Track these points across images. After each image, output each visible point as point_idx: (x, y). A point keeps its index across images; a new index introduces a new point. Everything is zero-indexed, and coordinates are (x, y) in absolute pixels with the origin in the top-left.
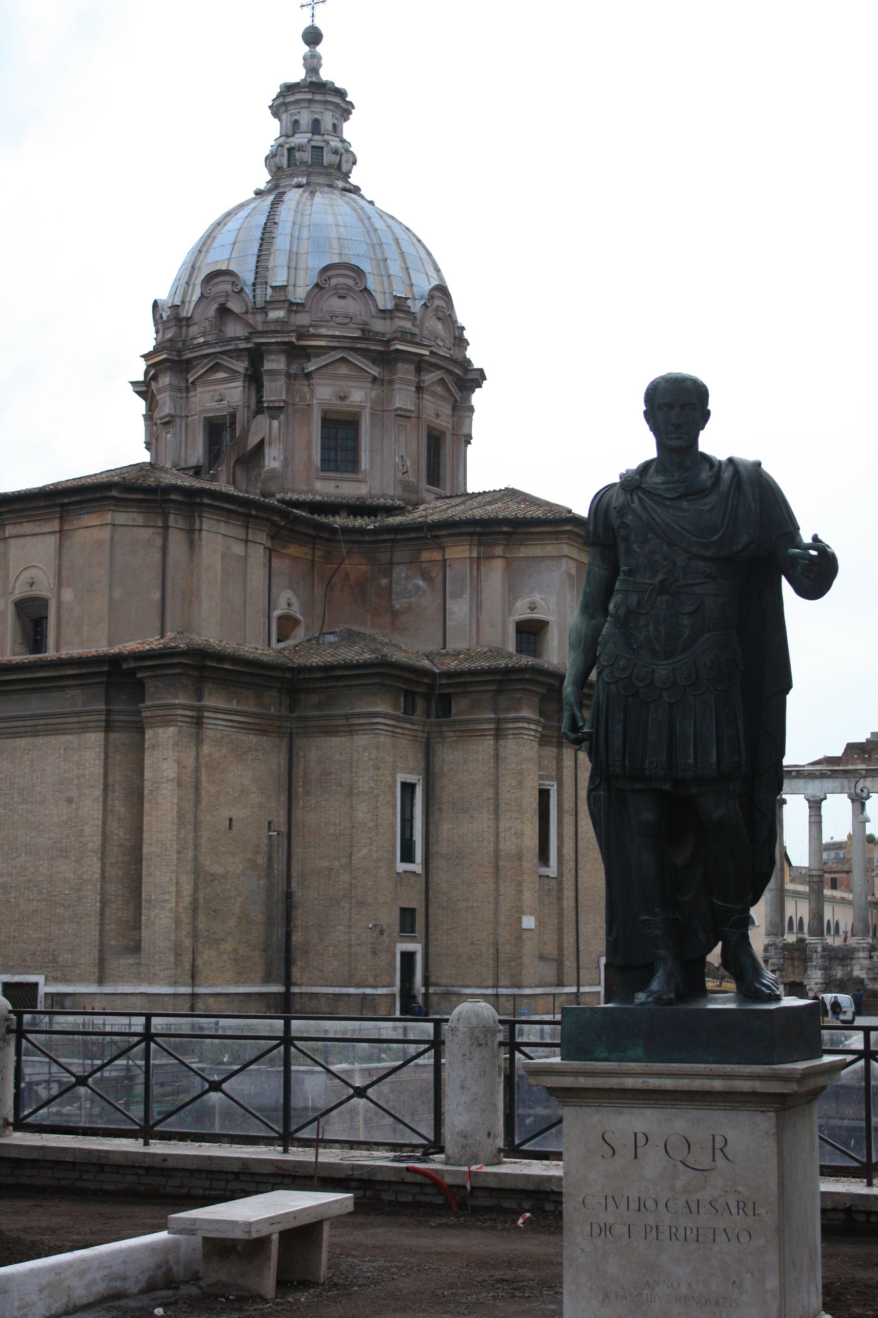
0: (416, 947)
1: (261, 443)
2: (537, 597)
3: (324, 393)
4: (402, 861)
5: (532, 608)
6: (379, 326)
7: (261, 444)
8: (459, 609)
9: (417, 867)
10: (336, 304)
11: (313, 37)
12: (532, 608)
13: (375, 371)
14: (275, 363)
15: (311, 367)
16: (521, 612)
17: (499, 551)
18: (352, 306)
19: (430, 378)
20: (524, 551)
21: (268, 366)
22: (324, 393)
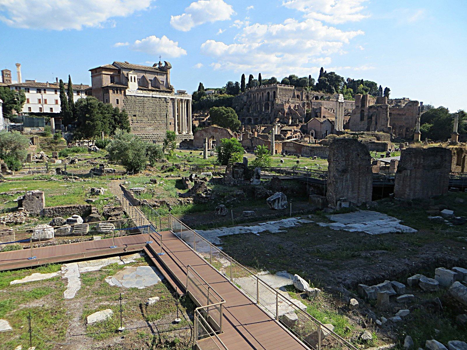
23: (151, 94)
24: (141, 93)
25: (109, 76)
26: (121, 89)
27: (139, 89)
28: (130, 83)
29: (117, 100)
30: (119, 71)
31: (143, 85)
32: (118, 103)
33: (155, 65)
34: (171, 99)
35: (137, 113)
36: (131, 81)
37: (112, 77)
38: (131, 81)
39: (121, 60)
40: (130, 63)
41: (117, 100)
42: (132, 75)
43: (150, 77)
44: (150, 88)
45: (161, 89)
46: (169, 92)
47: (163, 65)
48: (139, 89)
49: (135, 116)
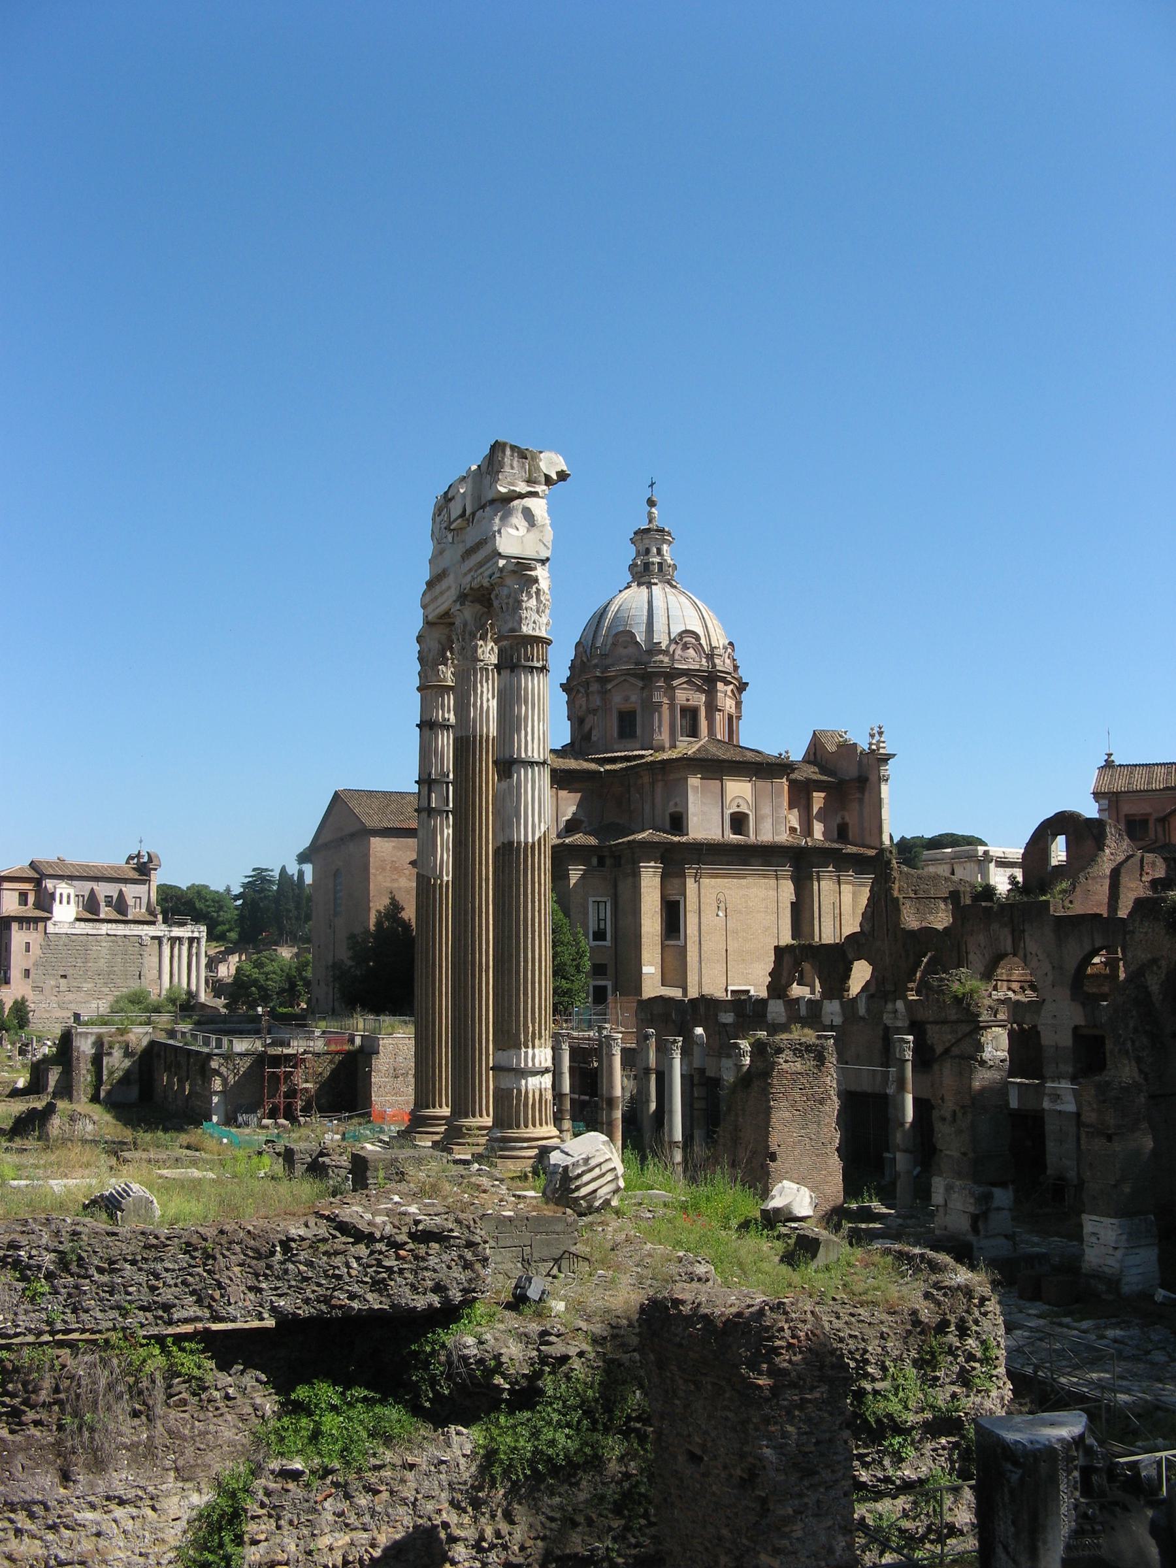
0: (609, 984)
1: (591, 729)
2: (677, 800)
3: (617, 700)
4: (605, 940)
5: (676, 804)
6: (645, 658)
7: (591, 729)
8: (647, 808)
9: (608, 943)
10: (621, 651)
11: (651, 503)
12: (676, 804)
13: (640, 684)
14: (595, 687)
15: (609, 687)
16: (672, 810)
17: (660, 777)
18: (631, 650)
19: (675, 683)
20: (672, 777)
21: (591, 689)
22: (617, 700)
23: (104, 928)
24: (87, 928)
25: (16, 894)
26: (37, 920)
27: (78, 920)
28: (57, 907)
29: (28, 944)
30: (38, 882)
31: (90, 909)
32: (28, 950)
33: (131, 858)
34: (153, 938)
35: (70, 972)
36: (61, 902)
37: (23, 896)
38: (61, 902)
39: (46, 855)
40: (71, 859)
41: (28, 944)
42: (63, 889)
43: (104, 890)
44: (102, 916)
45: (130, 917)
46: (153, 923)
47: (145, 859)
48: (78, 920)
49: (64, 977)
